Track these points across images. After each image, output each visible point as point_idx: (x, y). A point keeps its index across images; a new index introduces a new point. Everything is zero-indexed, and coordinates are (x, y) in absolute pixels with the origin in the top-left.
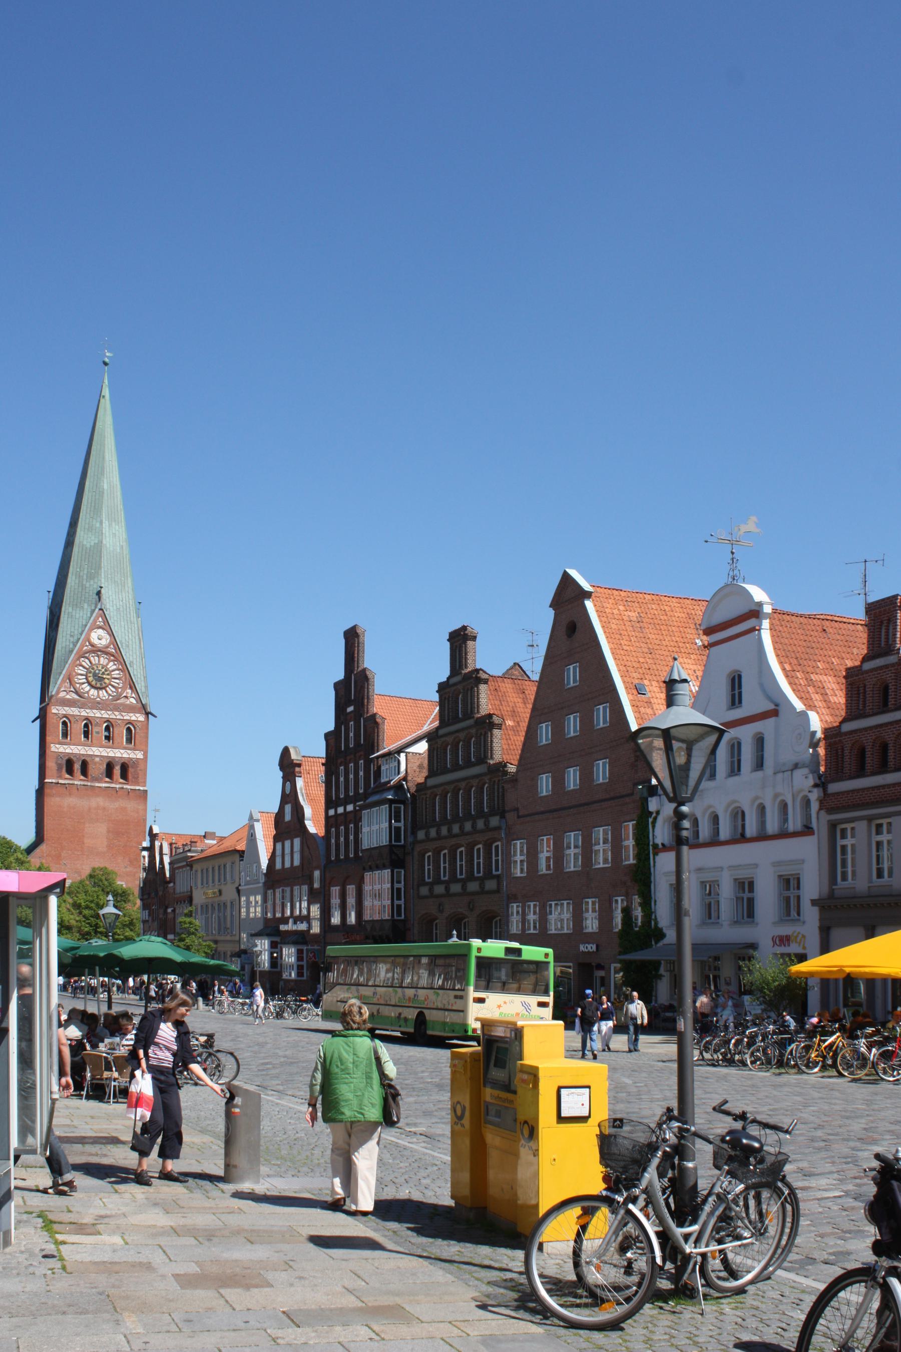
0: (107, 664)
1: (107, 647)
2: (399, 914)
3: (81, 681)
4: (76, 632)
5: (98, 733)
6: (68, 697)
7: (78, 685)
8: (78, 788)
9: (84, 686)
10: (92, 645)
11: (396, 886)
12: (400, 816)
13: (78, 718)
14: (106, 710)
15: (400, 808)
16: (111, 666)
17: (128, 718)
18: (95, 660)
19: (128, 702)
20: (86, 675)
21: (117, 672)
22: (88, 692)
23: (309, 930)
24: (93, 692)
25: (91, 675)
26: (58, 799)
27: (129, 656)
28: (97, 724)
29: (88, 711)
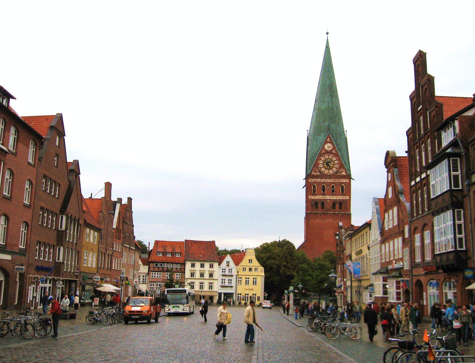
0: (332, 158)
1: (332, 150)
2: (461, 246)
3: (321, 167)
4: (318, 146)
5: (328, 189)
6: (316, 174)
7: (320, 169)
8: (321, 214)
9: (322, 169)
10: (325, 150)
12: (457, 167)
14: (332, 178)
15: (457, 160)
16: (334, 159)
17: (342, 181)
19: (342, 174)
21: (337, 161)
22: (324, 171)
23: (403, 268)
25: (325, 164)
28: (328, 185)
29: (324, 180)
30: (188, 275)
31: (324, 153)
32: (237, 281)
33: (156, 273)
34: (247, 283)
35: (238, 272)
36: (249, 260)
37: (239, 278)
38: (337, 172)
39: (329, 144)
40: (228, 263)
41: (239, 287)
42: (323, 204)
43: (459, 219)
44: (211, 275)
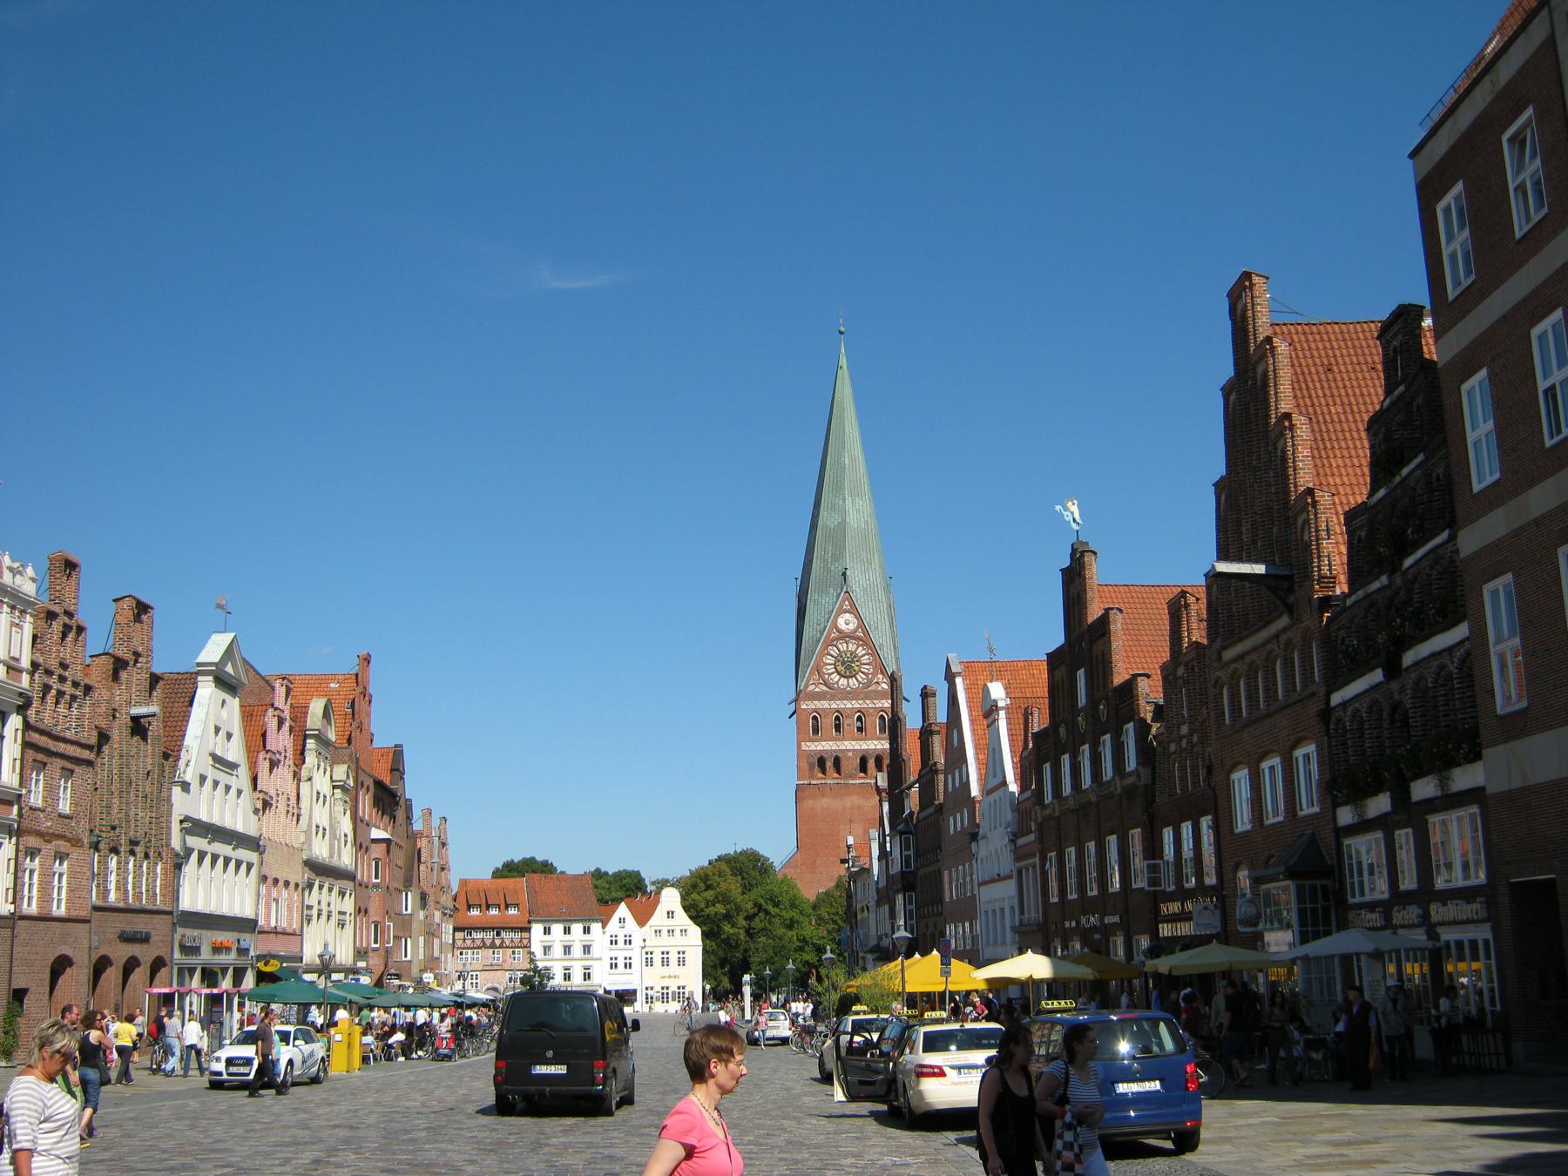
0: (856, 650)
1: (855, 631)
6: (817, 690)
9: (833, 676)
11: (908, 907)
14: (857, 699)
16: (860, 651)
18: (843, 647)
20: (834, 664)
21: (867, 657)
22: (837, 682)
24: (843, 681)
26: (810, 802)
27: (881, 637)
31: (837, 639)
34: (665, 962)
35: (644, 941)
36: (668, 913)
39: (847, 616)
40: (622, 920)
42: (837, 762)
43: (911, 904)
44: (587, 949)
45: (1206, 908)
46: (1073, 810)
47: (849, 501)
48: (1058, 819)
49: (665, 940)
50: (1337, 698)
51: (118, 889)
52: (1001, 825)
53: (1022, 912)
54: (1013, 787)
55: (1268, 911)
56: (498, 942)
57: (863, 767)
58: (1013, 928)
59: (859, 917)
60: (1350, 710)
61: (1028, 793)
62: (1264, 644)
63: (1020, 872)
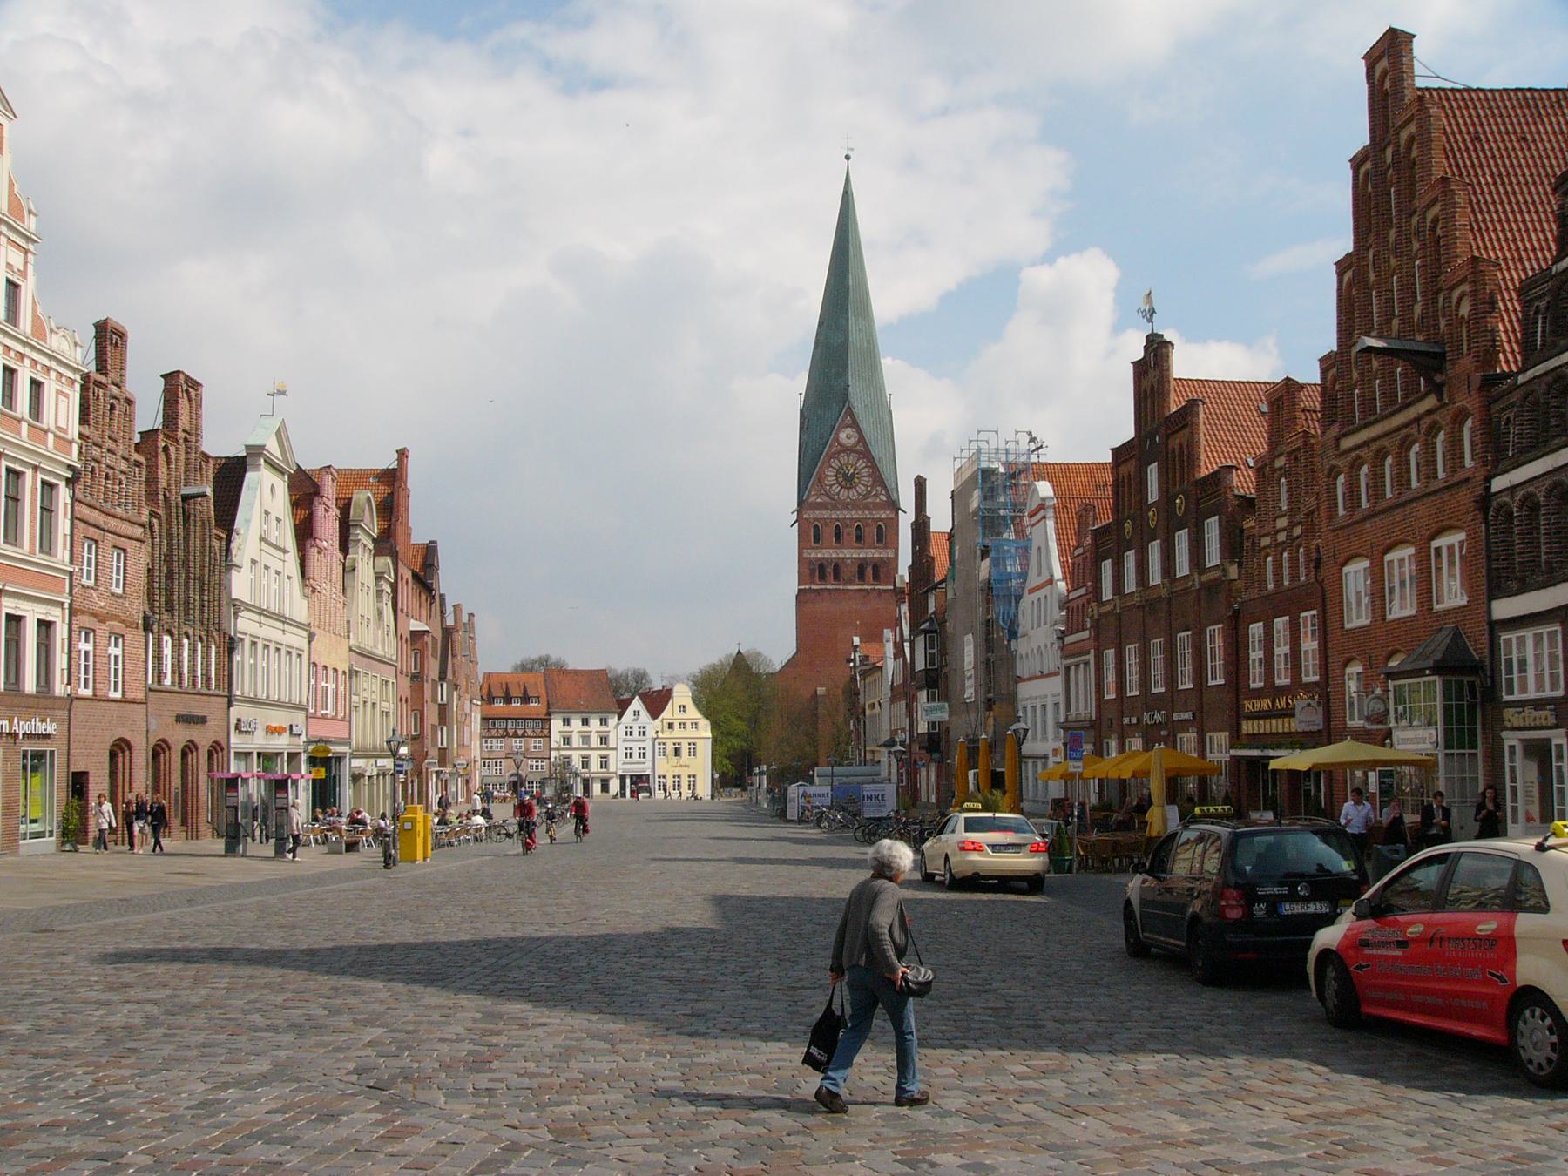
5: (848, 534)
6: (819, 500)
10: (839, 444)
13: (825, 522)
16: (861, 464)
24: (843, 493)
27: (876, 452)
28: (847, 526)
30: (556, 738)
31: (839, 453)
32: (657, 751)
33: (494, 740)
34: (677, 752)
37: (659, 744)
38: (866, 496)
39: (849, 430)
40: (637, 713)
41: (660, 760)
42: (837, 569)
44: (604, 740)
45: (1309, 705)
46: (1138, 607)
47: (851, 321)
48: (1119, 617)
49: (677, 732)
50: (1498, 484)
51: (173, 672)
52: (1045, 624)
53: (1068, 708)
54: (1062, 586)
55: (1401, 708)
56: (520, 732)
57: (861, 575)
58: (1058, 725)
59: (868, 712)
60: (1520, 494)
61: (1083, 591)
62: (1398, 429)
63: (1068, 669)
